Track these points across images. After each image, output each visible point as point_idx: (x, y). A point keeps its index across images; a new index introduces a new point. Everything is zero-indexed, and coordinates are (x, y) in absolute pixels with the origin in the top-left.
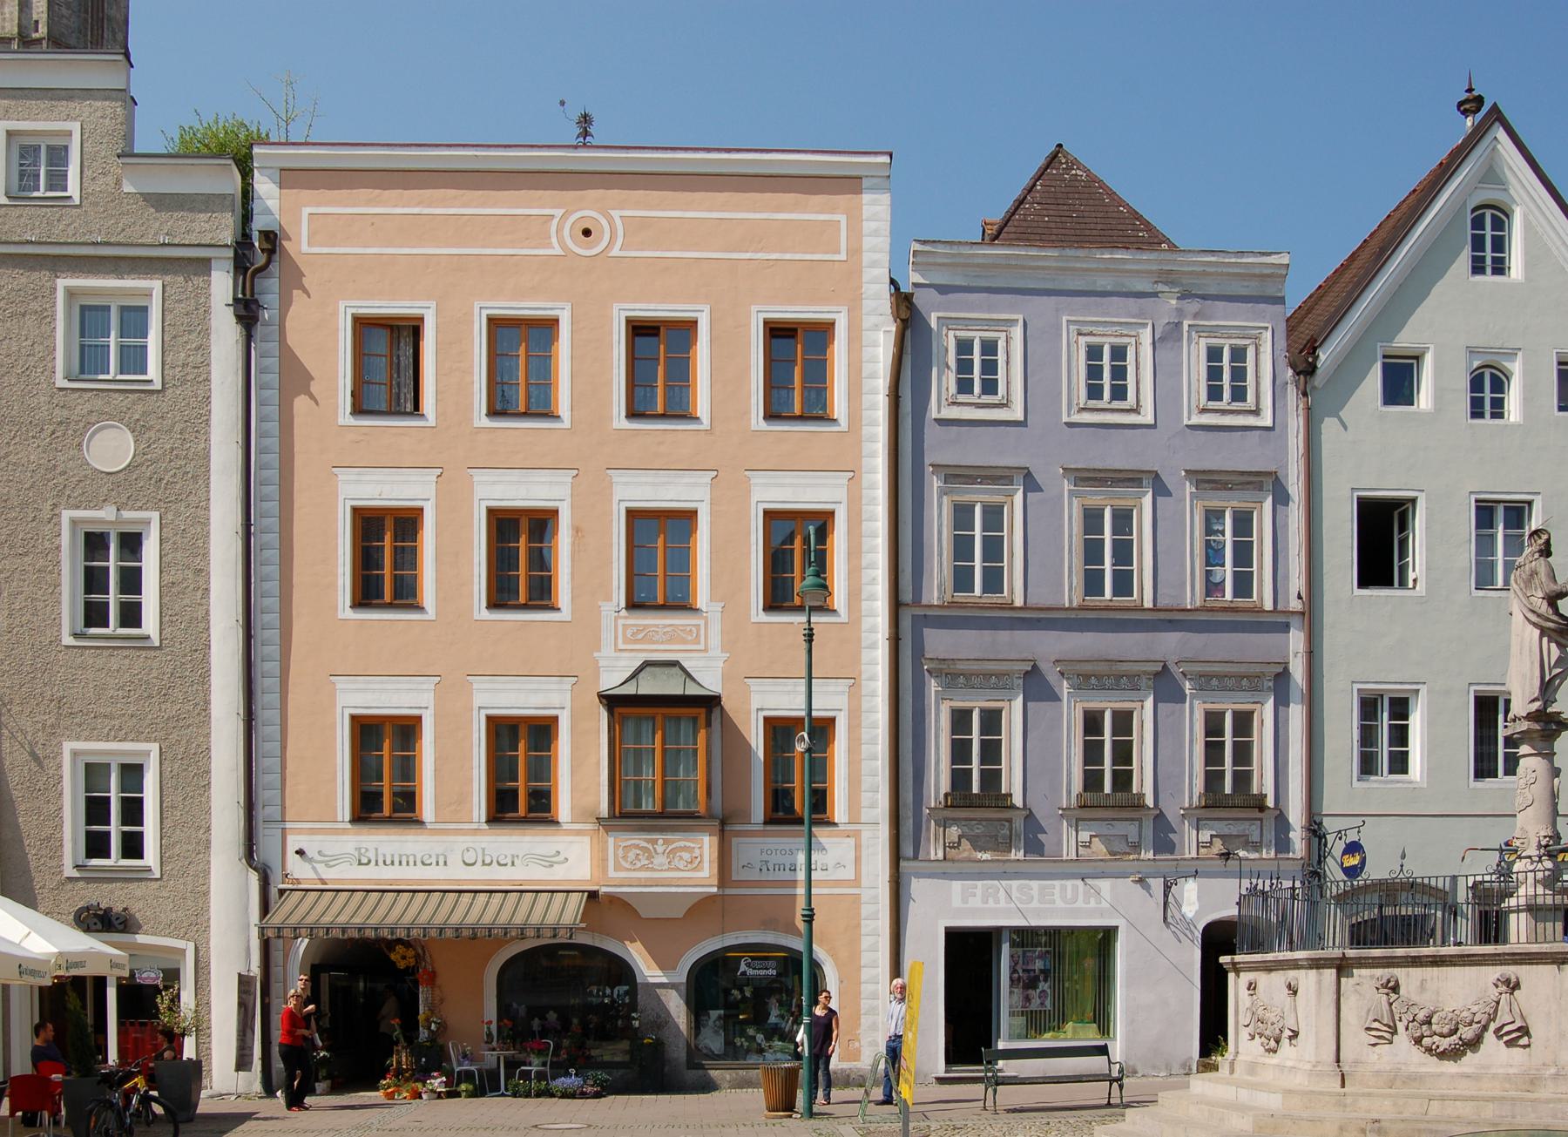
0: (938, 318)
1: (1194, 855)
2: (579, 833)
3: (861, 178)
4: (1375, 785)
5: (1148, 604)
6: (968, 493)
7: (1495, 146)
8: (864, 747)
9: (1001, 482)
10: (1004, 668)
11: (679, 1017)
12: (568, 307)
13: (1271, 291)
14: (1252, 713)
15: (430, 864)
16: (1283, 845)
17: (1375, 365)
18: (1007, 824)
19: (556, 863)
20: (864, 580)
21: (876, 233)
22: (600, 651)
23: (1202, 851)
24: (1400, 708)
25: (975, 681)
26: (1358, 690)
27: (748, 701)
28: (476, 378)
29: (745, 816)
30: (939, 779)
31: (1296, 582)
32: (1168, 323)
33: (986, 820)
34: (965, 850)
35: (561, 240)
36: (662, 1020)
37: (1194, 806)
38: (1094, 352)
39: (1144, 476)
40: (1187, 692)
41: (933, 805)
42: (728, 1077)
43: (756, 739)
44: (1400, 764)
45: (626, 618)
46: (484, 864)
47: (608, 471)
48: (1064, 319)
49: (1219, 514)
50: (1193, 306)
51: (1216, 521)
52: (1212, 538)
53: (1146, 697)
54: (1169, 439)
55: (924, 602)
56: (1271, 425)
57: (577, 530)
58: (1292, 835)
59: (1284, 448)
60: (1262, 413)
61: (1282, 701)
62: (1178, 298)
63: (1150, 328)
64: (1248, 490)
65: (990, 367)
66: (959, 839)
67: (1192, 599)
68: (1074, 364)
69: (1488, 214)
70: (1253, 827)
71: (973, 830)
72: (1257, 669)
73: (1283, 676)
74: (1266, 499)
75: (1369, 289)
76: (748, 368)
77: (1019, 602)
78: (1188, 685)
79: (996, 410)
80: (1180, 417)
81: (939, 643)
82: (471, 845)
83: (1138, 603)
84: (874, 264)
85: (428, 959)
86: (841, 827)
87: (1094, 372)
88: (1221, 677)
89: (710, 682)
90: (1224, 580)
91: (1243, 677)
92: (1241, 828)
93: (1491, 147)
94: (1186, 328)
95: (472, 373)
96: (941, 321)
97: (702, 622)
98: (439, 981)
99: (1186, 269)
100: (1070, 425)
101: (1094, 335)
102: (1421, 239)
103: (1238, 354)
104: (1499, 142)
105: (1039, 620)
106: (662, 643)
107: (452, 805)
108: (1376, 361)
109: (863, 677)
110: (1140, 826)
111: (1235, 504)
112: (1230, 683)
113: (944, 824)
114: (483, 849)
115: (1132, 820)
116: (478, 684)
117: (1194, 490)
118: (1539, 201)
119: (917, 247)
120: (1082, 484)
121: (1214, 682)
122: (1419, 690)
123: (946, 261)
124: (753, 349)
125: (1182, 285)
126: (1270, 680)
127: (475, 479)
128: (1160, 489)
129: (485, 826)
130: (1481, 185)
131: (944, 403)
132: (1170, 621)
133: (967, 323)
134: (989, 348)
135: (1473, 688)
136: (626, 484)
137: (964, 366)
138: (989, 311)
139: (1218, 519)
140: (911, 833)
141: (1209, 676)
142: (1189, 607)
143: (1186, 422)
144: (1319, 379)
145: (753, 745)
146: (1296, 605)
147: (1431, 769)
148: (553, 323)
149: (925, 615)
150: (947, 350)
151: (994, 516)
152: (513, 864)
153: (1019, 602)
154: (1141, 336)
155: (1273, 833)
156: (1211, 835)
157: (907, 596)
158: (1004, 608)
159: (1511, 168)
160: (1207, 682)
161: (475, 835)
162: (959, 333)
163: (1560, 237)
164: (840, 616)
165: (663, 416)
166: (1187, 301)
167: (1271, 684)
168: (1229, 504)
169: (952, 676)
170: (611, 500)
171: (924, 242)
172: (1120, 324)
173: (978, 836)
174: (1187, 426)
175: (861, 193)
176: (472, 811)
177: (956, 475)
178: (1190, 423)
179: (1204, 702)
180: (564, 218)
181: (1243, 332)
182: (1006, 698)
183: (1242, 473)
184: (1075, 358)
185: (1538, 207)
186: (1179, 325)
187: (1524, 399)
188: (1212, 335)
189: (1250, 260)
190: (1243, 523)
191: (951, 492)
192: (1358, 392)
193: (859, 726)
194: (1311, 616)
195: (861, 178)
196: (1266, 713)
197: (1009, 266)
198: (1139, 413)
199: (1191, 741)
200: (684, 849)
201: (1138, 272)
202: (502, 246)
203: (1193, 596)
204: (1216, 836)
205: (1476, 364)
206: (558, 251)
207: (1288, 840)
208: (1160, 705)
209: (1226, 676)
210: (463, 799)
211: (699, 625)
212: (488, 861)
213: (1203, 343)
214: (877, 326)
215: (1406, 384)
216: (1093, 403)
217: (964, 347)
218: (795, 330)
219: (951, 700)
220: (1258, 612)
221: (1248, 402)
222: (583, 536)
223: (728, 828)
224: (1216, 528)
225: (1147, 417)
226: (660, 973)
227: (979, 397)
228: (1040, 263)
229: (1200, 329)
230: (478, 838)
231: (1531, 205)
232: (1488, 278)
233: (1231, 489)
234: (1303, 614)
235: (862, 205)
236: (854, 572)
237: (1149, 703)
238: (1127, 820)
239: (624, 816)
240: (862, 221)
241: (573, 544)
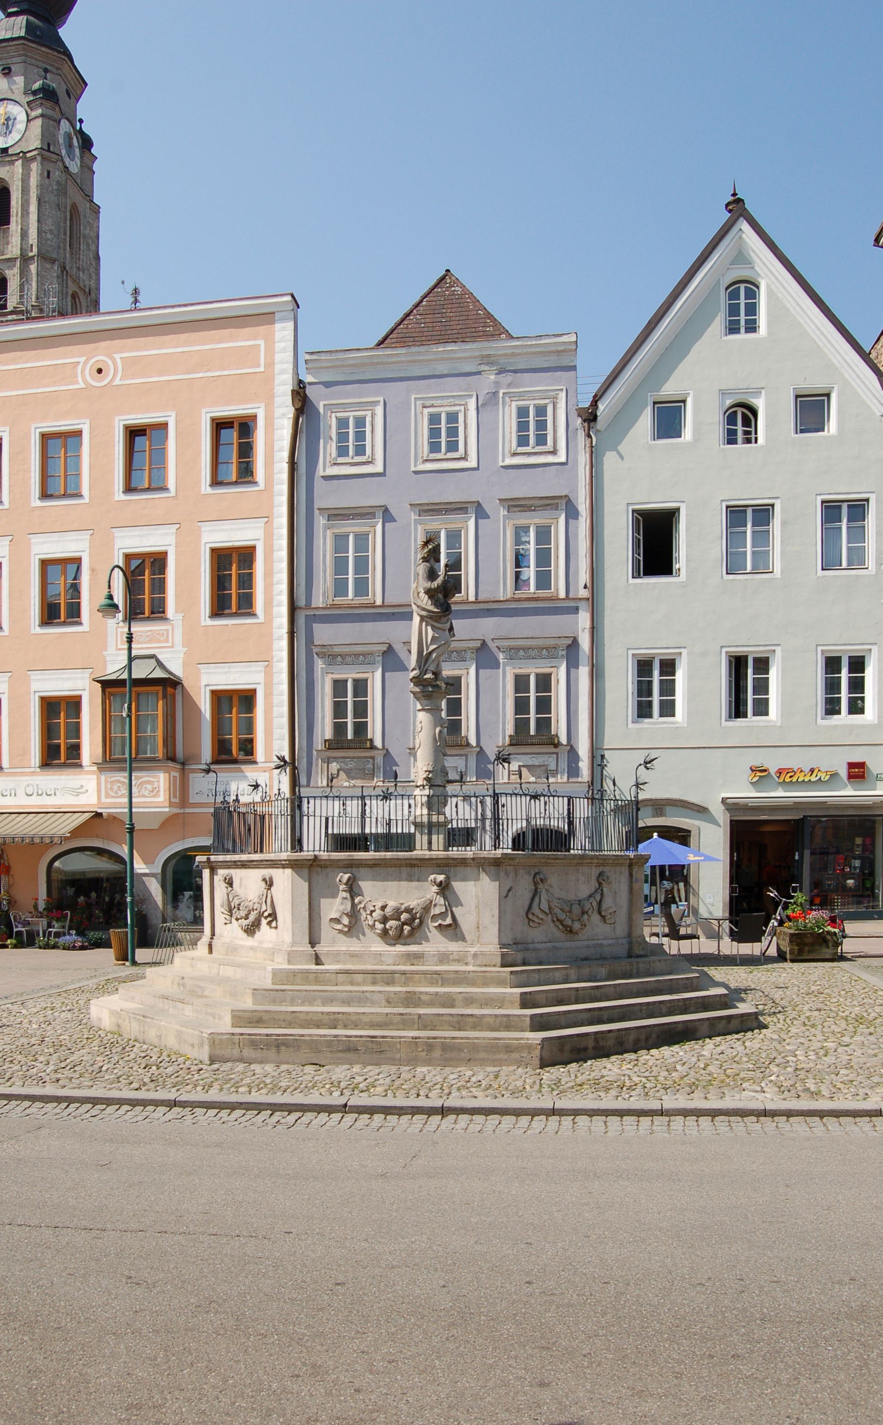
0: (324, 405)
1: (506, 780)
2: (93, 773)
3: (274, 313)
4: (646, 726)
5: (472, 598)
6: (344, 526)
7: (741, 236)
8: (275, 709)
9: (367, 517)
10: (366, 649)
11: (157, 896)
12: (88, 422)
13: (566, 362)
14: (551, 674)
15: (6, 796)
16: (573, 771)
17: (646, 410)
18: (371, 760)
19: (81, 793)
20: (274, 593)
21: (283, 350)
22: (106, 650)
23: (512, 777)
24: (668, 667)
25: (348, 659)
26: (633, 655)
27: (199, 680)
28: (33, 475)
29: (197, 758)
30: (325, 729)
31: (583, 576)
32: (488, 393)
33: (357, 758)
34: (342, 780)
35: (84, 378)
36: (147, 897)
37: (507, 744)
38: (434, 419)
39: (469, 505)
40: (501, 661)
41: (320, 748)
42: (188, 938)
43: (205, 706)
44: (668, 709)
45: (123, 627)
46: (38, 795)
47: (112, 530)
48: (413, 397)
49: (526, 529)
50: (508, 378)
51: (524, 534)
52: (521, 547)
53: (471, 666)
54: (488, 477)
55: (313, 606)
56: (565, 461)
57: (93, 570)
58: (581, 764)
59: (576, 477)
60: (558, 453)
61: (573, 664)
62: (496, 374)
63: (474, 399)
64: (547, 510)
65: (360, 436)
66: (338, 772)
67: (504, 593)
68: (420, 428)
69: (742, 287)
70: (551, 759)
71: (347, 765)
72: (552, 642)
73: (574, 645)
74: (560, 515)
75: (637, 355)
76: (200, 452)
77: (379, 602)
78: (501, 657)
79: (364, 466)
80: (496, 459)
81: (324, 634)
82: (29, 782)
83: (465, 598)
84: (282, 372)
85: (6, 858)
86: (260, 765)
87: (434, 433)
88: (525, 649)
89: (176, 668)
90: (529, 578)
91: (543, 649)
92: (541, 760)
93: (737, 237)
94: (501, 395)
95: (30, 472)
96: (326, 407)
97: (170, 628)
98: (12, 872)
99: (500, 352)
100: (416, 473)
101: (435, 407)
102: (679, 313)
103: (541, 411)
104: (743, 233)
105: (393, 614)
106: (145, 643)
107: (19, 754)
108: (647, 406)
109: (275, 660)
110: (466, 760)
111: (537, 521)
112: (533, 653)
113: (328, 761)
114: (37, 785)
115: (461, 755)
116: (34, 676)
117: (506, 513)
118: (776, 274)
119: (308, 357)
120: (424, 514)
121: (522, 653)
122: (681, 653)
123: (329, 364)
124: (203, 439)
125: (499, 364)
126: (563, 650)
127: (32, 541)
128: (481, 513)
129: (38, 770)
130: (732, 266)
131: (328, 464)
132: (488, 610)
133: (344, 407)
134: (360, 422)
135: (724, 650)
136: (123, 537)
137: (342, 437)
138: (360, 397)
139: (526, 533)
140: (305, 769)
141: (518, 649)
142: (502, 599)
143: (501, 464)
144: (601, 423)
145: (203, 710)
146: (584, 593)
147: (690, 714)
148: (78, 434)
149: (314, 615)
150: (330, 427)
151: (362, 541)
152: (55, 794)
153: (379, 602)
154: (468, 404)
155: (566, 763)
156: (519, 766)
157: (301, 602)
158: (368, 607)
159: (753, 251)
160: (514, 653)
161: (32, 776)
162: (338, 415)
163: (795, 300)
164: (258, 618)
165: (149, 489)
166: (502, 375)
167: (564, 653)
168: (533, 520)
169: (332, 657)
170: (113, 549)
171: (312, 353)
172: (453, 396)
173: (351, 770)
174: (501, 466)
175: (274, 323)
176: (30, 760)
177: (336, 515)
178: (503, 464)
179: (514, 668)
180: (86, 362)
181: (544, 394)
182: (370, 671)
183: (542, 498)
184: (421, 424)
185: (777, 279)
186: (495, 393)
187: (766, 426)
188: (521, 398)
189: (547, 341)
190: (544, 535)
191: (333, 526)
192: (632, 431)
193: (272, 694)
194: (595, 602)
195: (274, 313)
196: (560, 676)
197: (372, 364)
198: (467, 460)
199: (504, 697)
200: (148, 782)
201: (465, 358)
202: (48, 386)
203: (505, 590)
204: (523, 766)
205: (729, 402)
206: (82, 385)
207: (578, 768)
208: (481, 671)
209: (530, 648)
210: (25, 752)
211: (168, 630)
212: (40, 793)
213: (514, 404)
214: (284, 415)
215: (677, 421)
216: (433, 456)
217: (343, 423)
218: (233, 422)
219: (332, 673)
220: (553, 600)
221: (548, 444)
222: (97, 574)
223: (186, 767)
224: (524, 539)
225: (472, 463)
226: (144, 866)
227: (352, 458)
228: (394, 360)
229: (511, 395)
230: (35, 778)
231: (773, 279)
232: (743, 336)
233: (534, 510)
234: (588, 599)
235: (275, 331)
236: (269, 587)
237: (473, 670)
238: (457, 755)
239: (112, 761)
240: (275, 343)
241: (90, 579)
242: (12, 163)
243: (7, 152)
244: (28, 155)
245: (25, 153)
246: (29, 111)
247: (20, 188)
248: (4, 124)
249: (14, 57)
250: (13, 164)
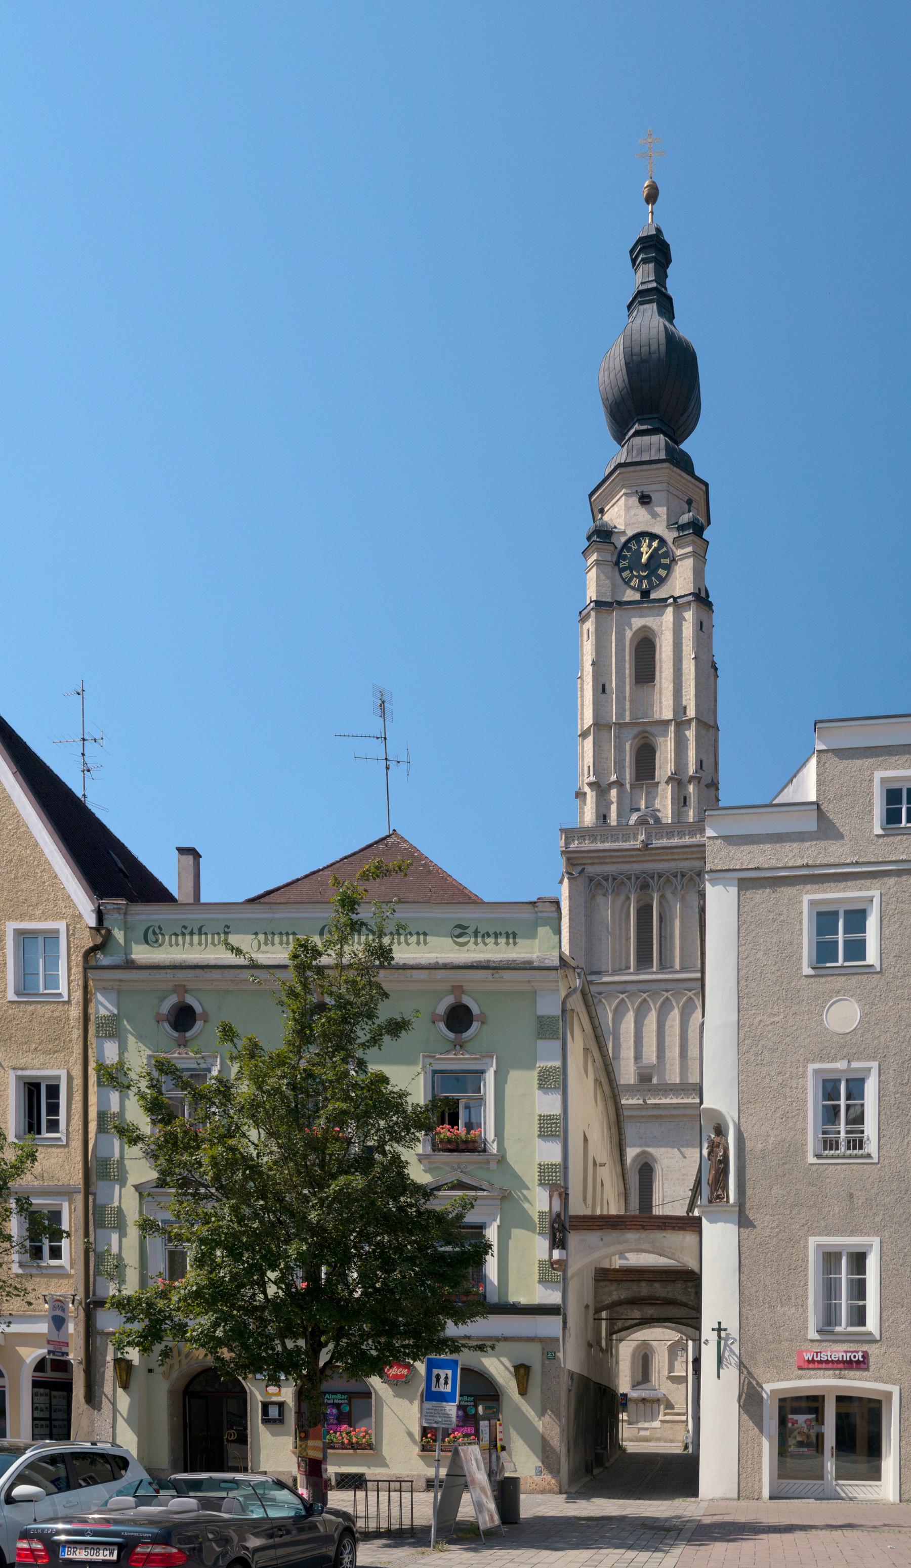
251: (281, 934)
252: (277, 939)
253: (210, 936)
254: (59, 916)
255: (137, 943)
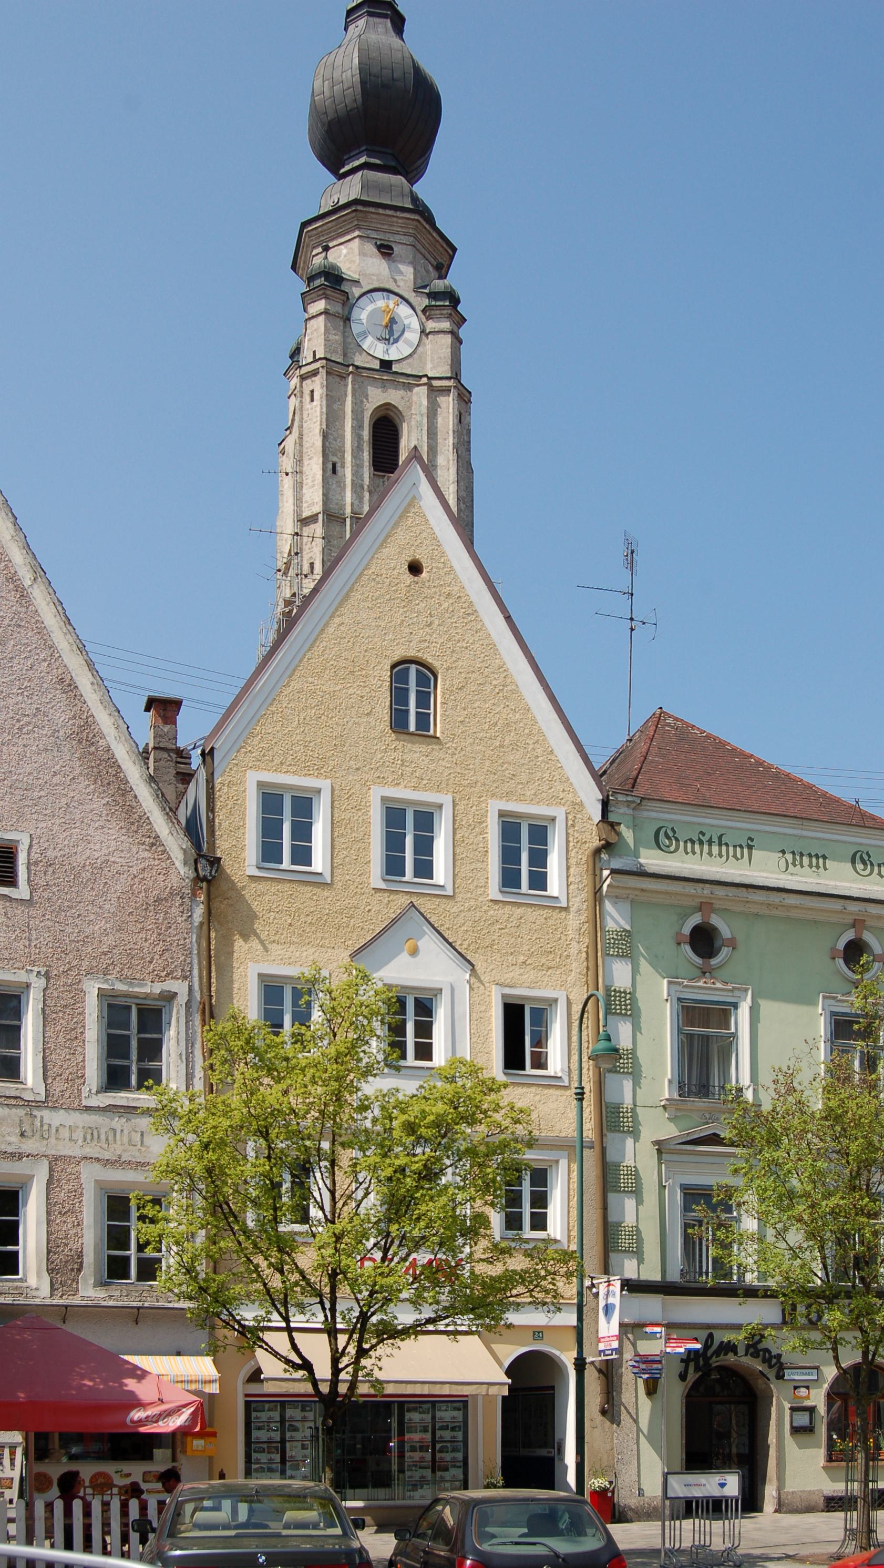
242: (409, 387)
243: (391, 368)
244: (436, 383)
245: (429, 378)
246: (423, 318)
247: (425, 428)
248: (386, 326)
249: (398, 233)
250: (411, 391)
251: (810, 855)
252: (806, 860)
253: (731, 849)
254: (556, 800)
255: (648, 847)
